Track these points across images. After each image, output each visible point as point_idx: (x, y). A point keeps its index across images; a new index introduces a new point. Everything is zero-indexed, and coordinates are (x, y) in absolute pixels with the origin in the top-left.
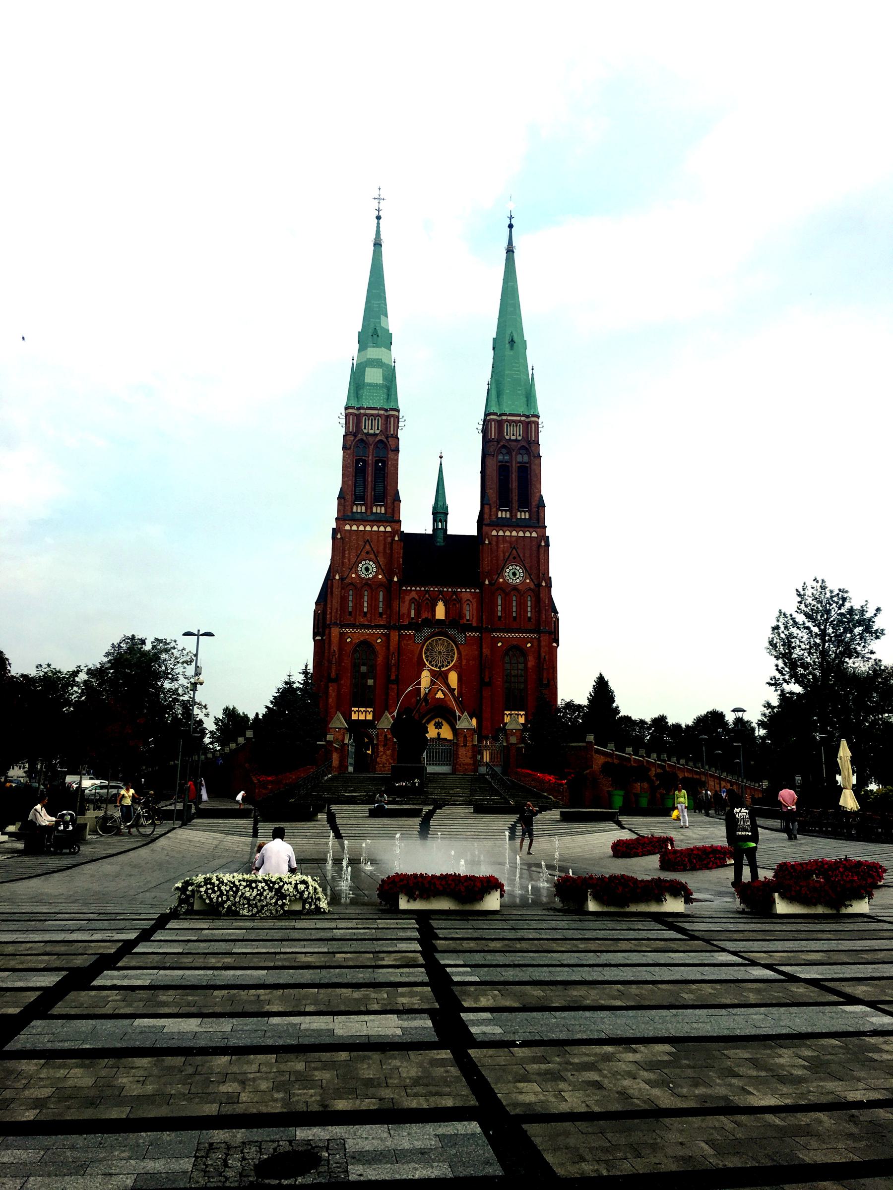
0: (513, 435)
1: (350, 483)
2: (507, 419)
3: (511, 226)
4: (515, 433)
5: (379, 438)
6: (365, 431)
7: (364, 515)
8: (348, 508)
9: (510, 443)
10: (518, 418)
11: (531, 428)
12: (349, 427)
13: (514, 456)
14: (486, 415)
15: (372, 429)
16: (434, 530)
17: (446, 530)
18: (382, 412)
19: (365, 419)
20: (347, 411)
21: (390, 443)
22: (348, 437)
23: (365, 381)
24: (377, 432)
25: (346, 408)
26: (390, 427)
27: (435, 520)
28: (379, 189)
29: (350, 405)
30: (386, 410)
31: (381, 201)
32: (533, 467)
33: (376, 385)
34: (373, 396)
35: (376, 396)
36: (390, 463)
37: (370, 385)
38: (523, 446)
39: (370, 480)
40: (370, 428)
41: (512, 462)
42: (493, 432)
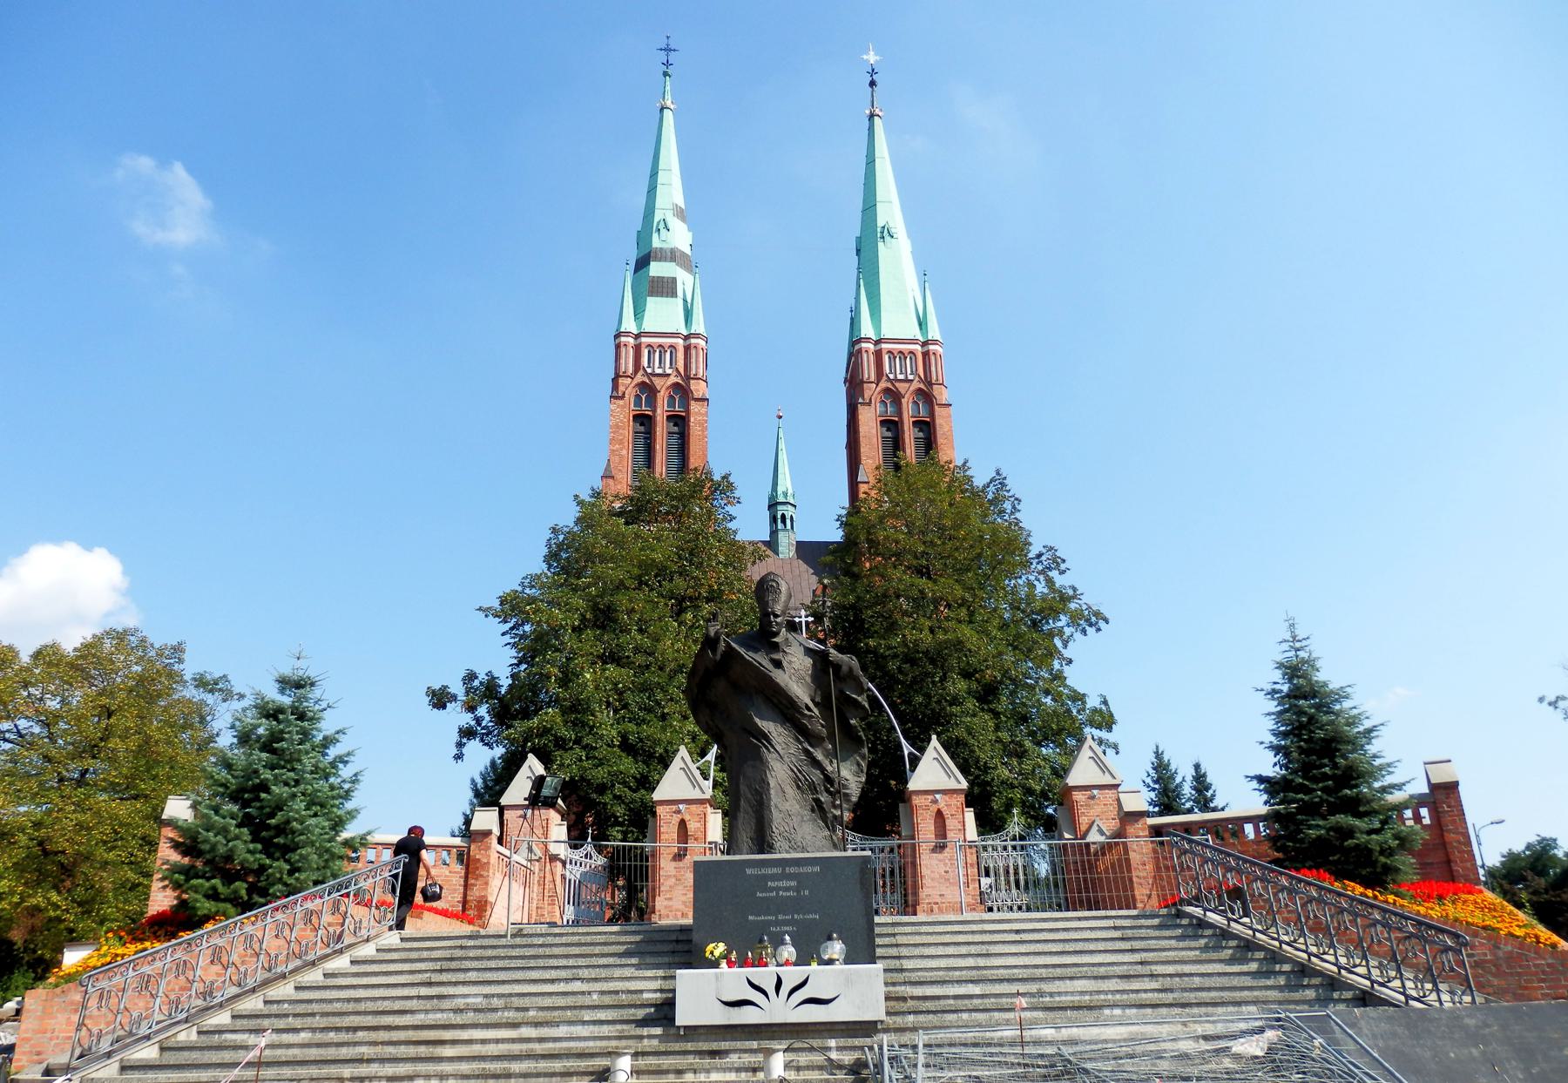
0: (901, 373)
1: (624, 452)
5: (673, 379)
9: (897, 384)
36: (692, 419)
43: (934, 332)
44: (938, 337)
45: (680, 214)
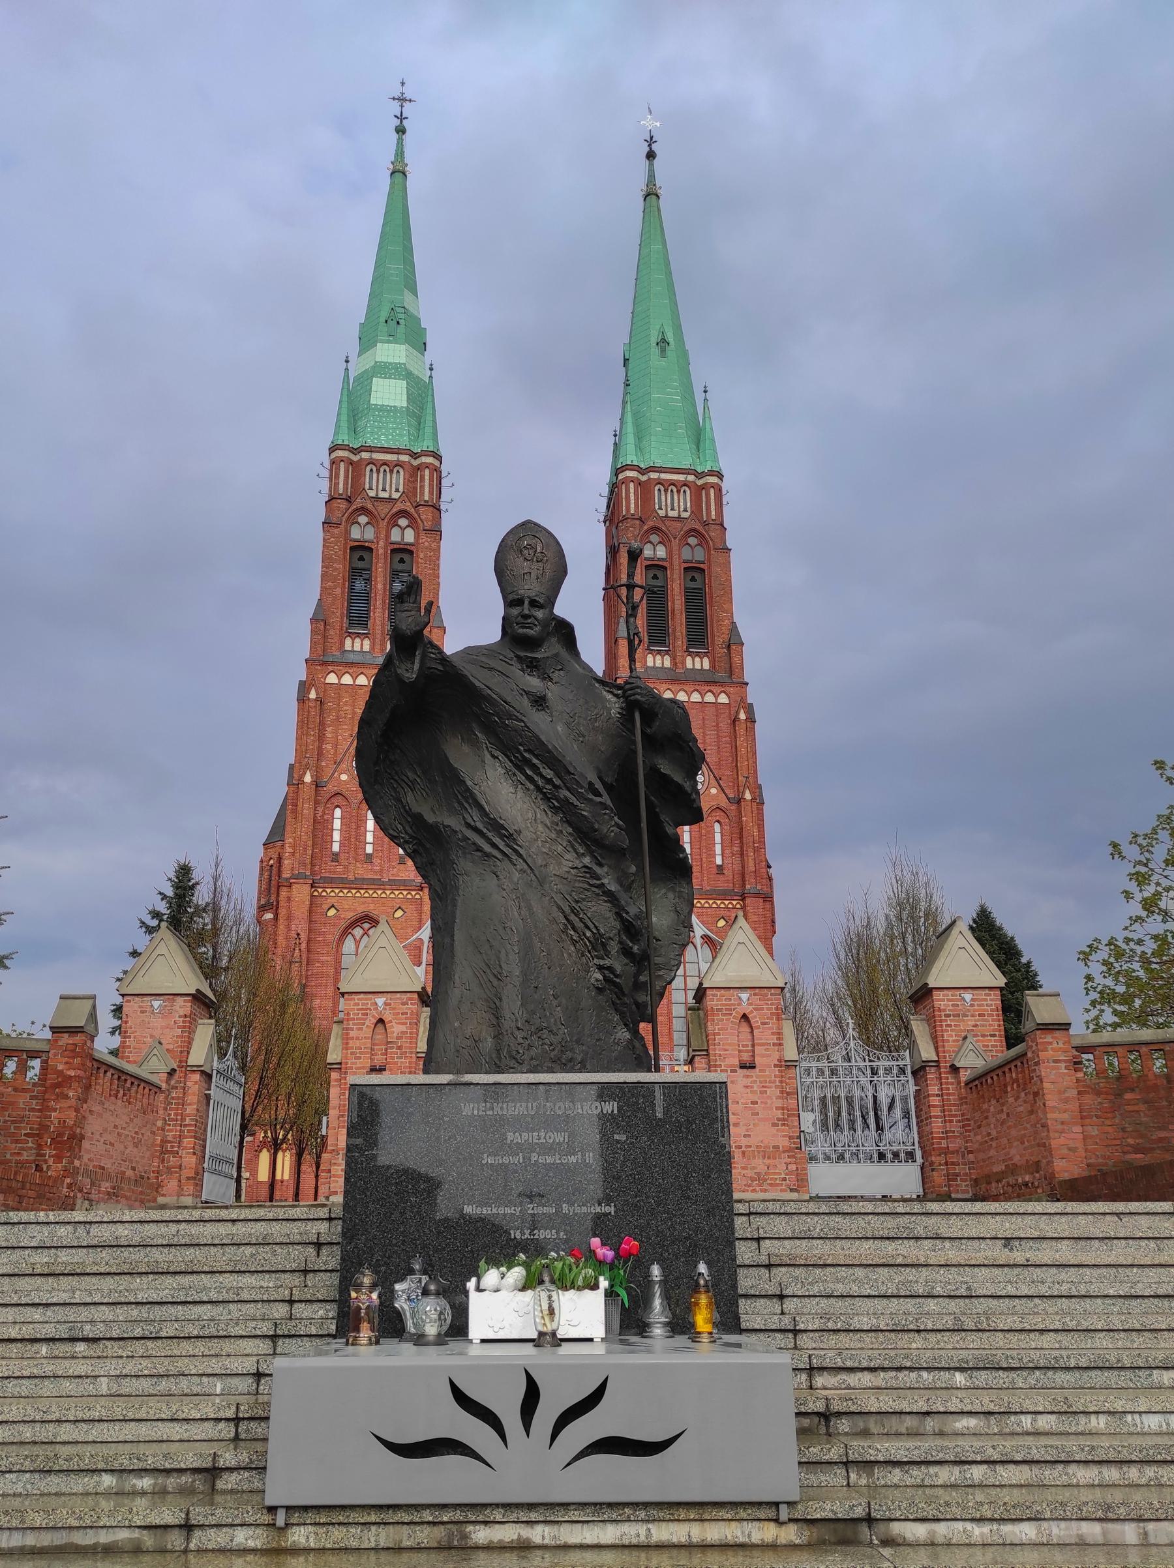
0: (673, 509)
1: (338, 591)
2: (659, 479)
4: (676, 505)
5: (399, 506)
6: (372, 493)
7: (369, 656)
8: (334, 641)
9: (667, 523)
10: (681, 477)
11: (708, 496)
12: (337, 484)
13: (675, 548)
14: (617, 472)
15: (384, 490)
18: (405, 458)
19: (371, 470)
20: (334, 455)
21: (423, 517)
22: (335, 504)
23: (373, 401)
24: (396, 495)
25: (332, 450)
26: (422, 487)
29: (340, 442)
30: (415, 456)
32: (716, 569)
33: (395, 409)
34: (386, 428)
35: (394, 429)
36: (422, 555)
37: (382, 408)
38: (694, 530)
39: (380, 586)
40: (381, 487)
41: (671, 558)
42: (632, 502)
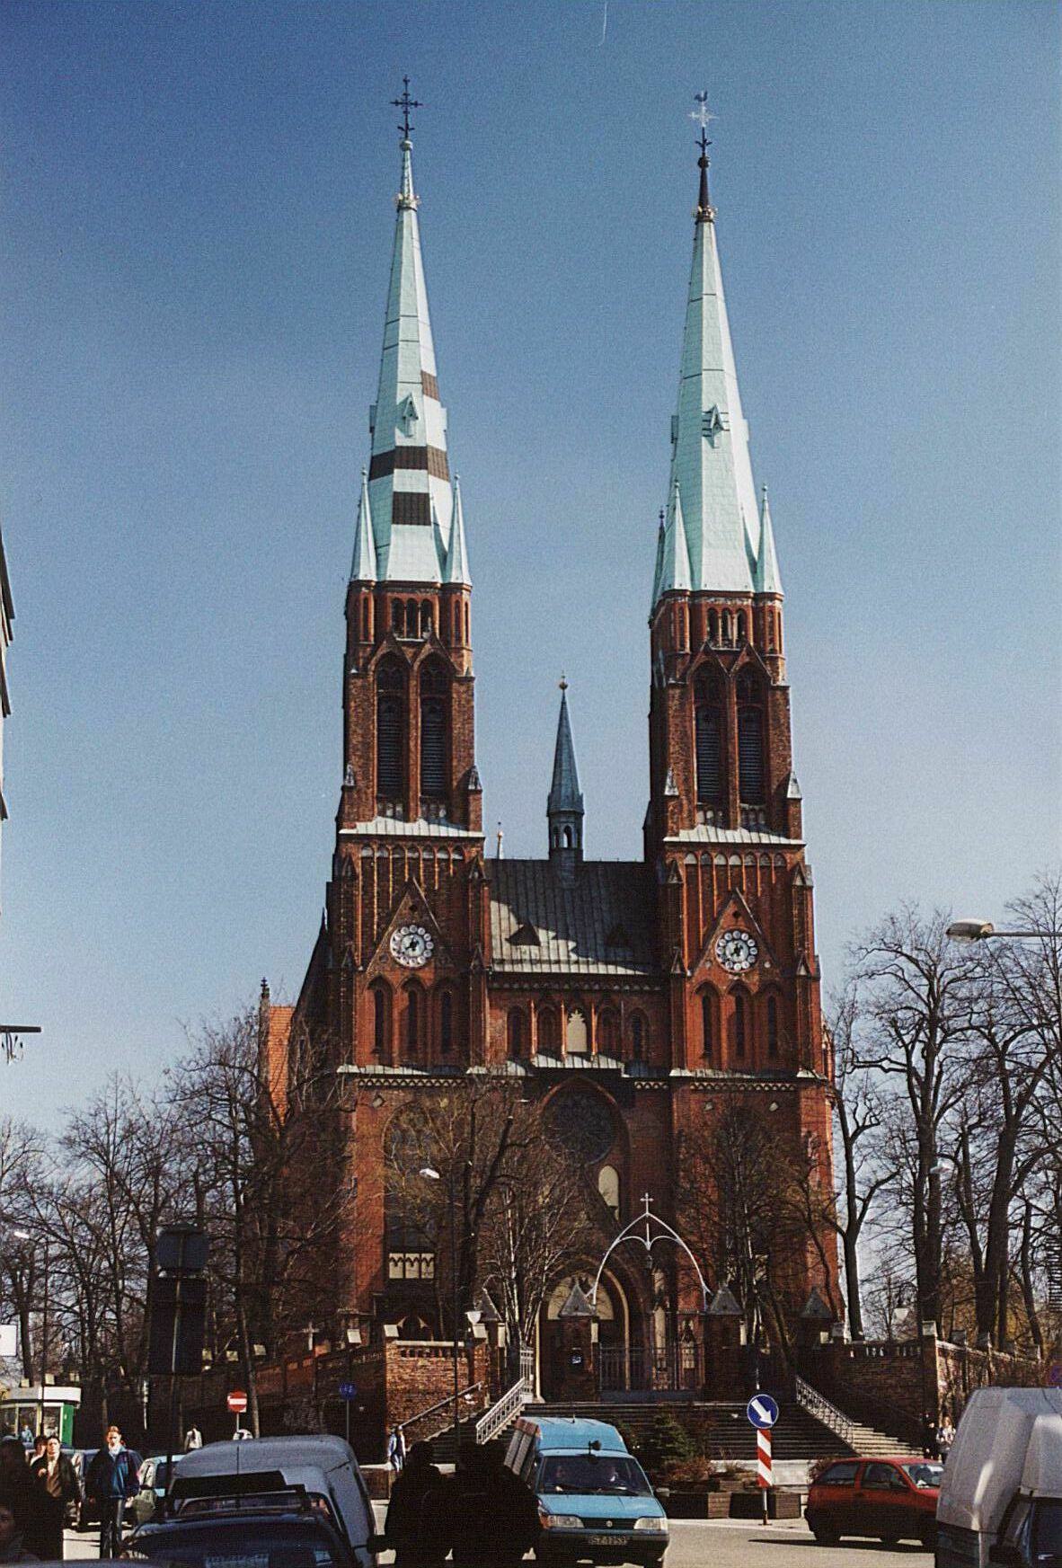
3: (703, 163)
16: (551, 852)
17: (581, 852)
27: (554, 833)
28: (406, 81)
31: (412, 109)
43: (772, 583)
44: (778, 589)
45: (428, 385)
